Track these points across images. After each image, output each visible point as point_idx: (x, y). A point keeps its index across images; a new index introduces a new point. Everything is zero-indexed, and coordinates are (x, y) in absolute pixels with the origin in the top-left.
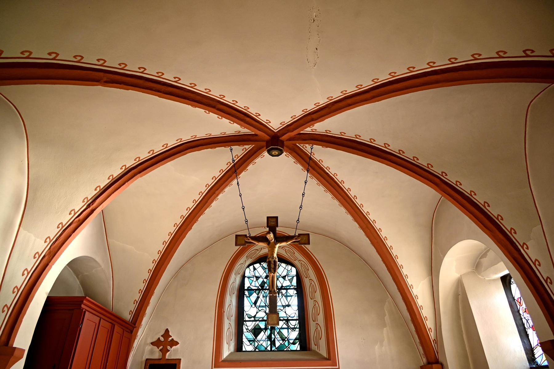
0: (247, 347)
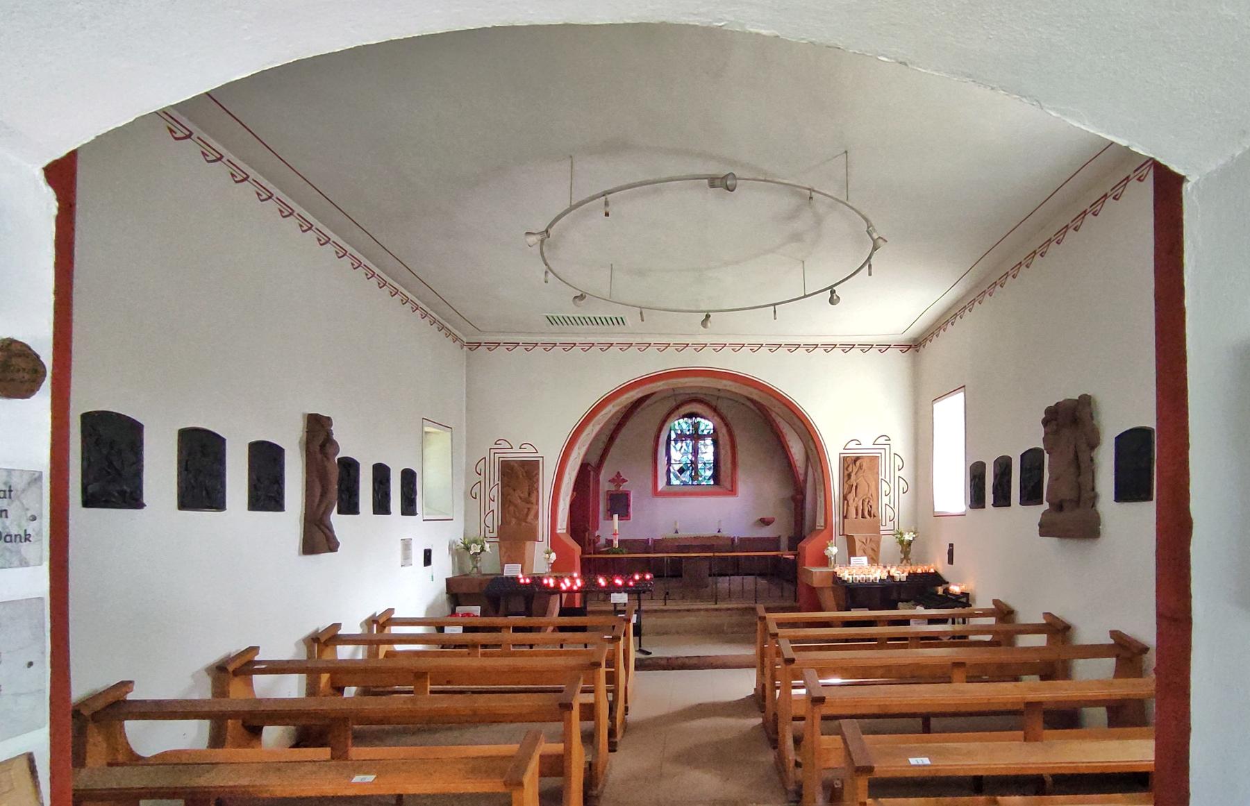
0: (674, 482)
